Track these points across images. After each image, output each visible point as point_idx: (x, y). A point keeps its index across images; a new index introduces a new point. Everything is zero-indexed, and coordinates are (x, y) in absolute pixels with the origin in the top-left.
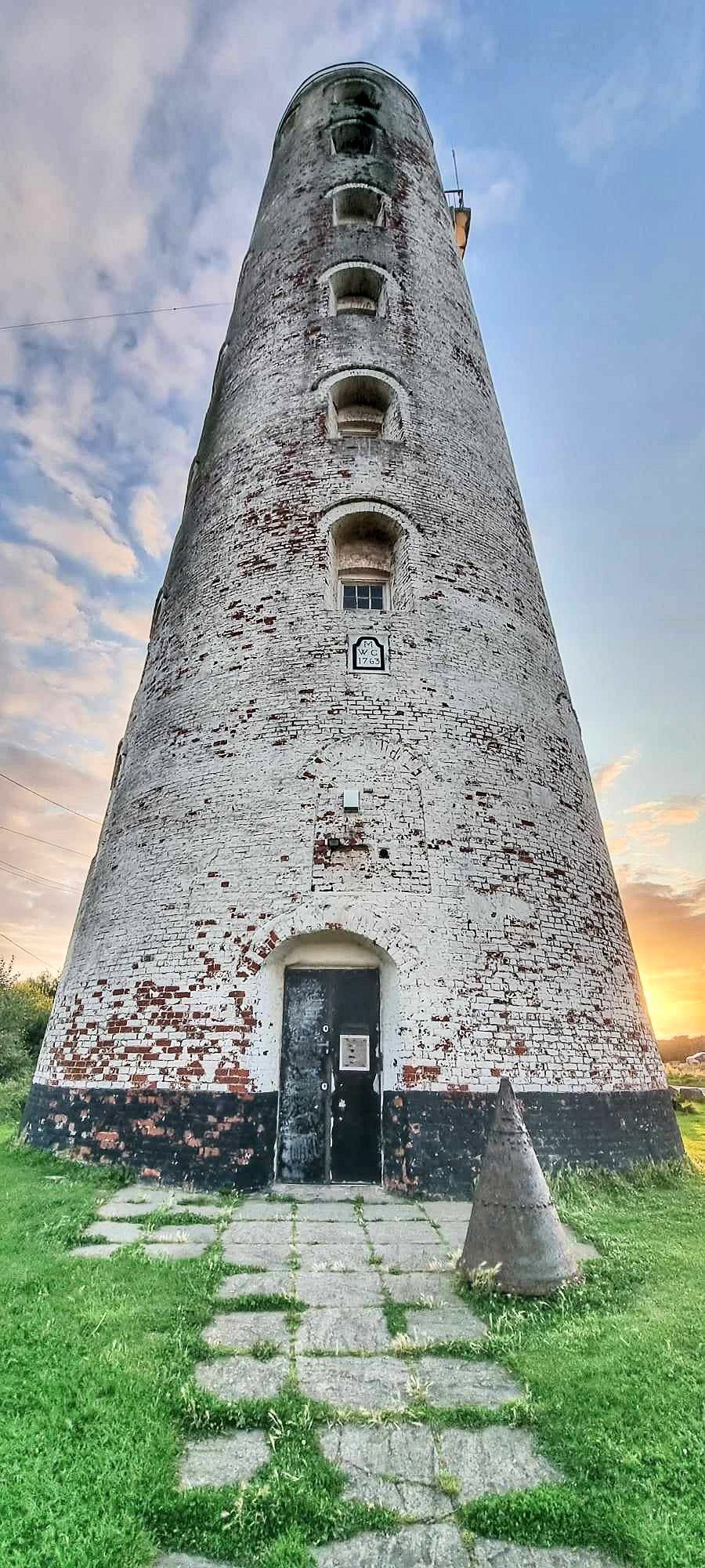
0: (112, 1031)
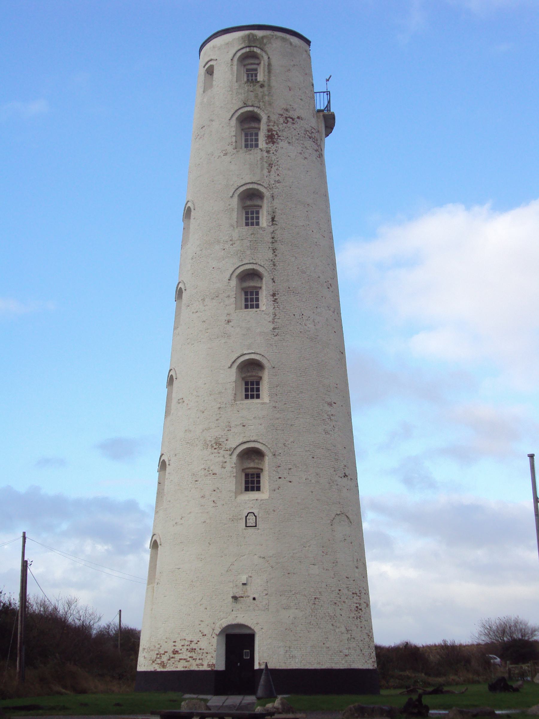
0: (174, 654)
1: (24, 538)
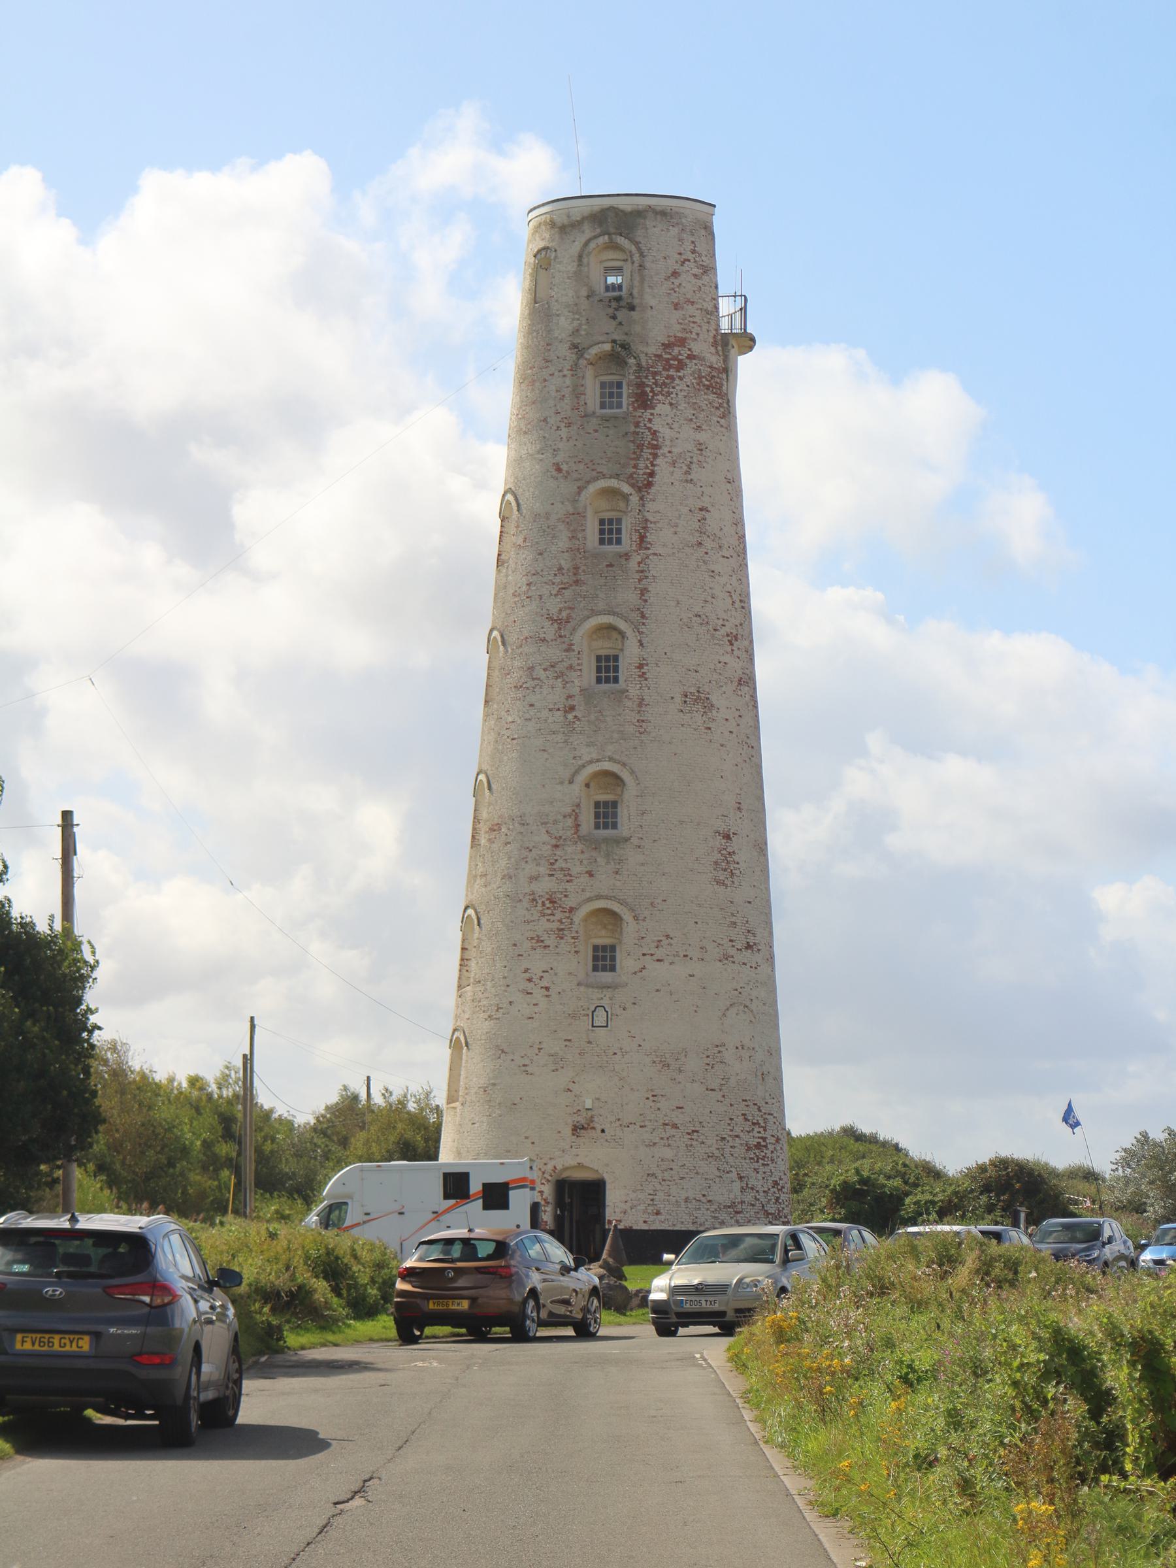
1: (253, 1027)
